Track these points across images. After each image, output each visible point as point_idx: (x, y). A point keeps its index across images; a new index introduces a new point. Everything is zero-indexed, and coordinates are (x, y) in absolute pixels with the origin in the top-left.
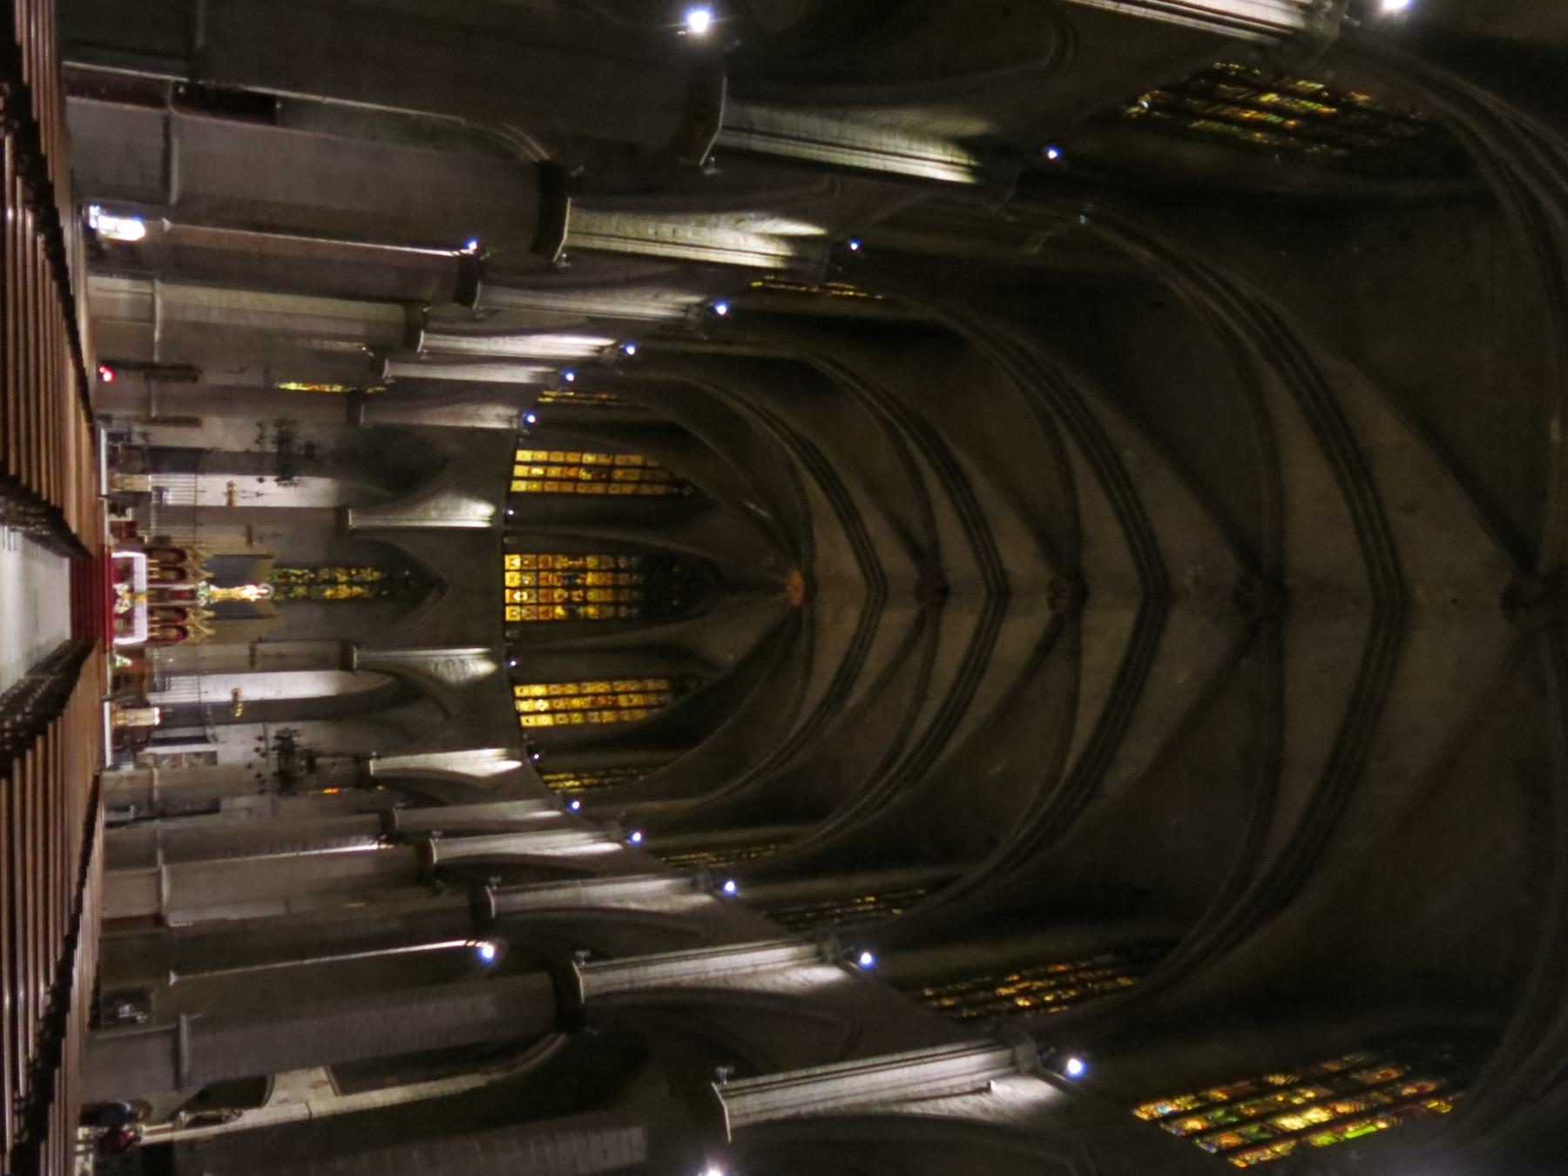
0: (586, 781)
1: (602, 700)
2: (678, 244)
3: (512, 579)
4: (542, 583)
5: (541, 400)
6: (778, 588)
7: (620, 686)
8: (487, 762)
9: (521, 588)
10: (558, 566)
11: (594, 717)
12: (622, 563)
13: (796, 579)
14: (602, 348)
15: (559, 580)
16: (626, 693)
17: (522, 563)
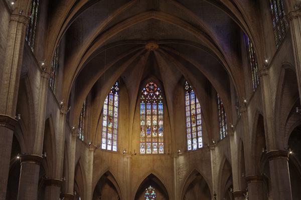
0: (223, 124)
1: (193, 119)
2: (11, 72)
3: (149, 151)
4: (150, 140)
5: (83, 140)
6: (152, 53)
7: (188, 114)
8: (215, 156)
9: (152, 148)
10: (144, 135)
11: (199, 122)
12: (142, 112)
13: (150, 46)
14: (61, 114)
15: (149, 135)
16: (190, 111)
17: (143, 148)
